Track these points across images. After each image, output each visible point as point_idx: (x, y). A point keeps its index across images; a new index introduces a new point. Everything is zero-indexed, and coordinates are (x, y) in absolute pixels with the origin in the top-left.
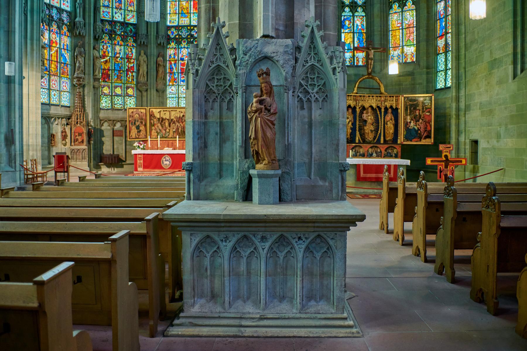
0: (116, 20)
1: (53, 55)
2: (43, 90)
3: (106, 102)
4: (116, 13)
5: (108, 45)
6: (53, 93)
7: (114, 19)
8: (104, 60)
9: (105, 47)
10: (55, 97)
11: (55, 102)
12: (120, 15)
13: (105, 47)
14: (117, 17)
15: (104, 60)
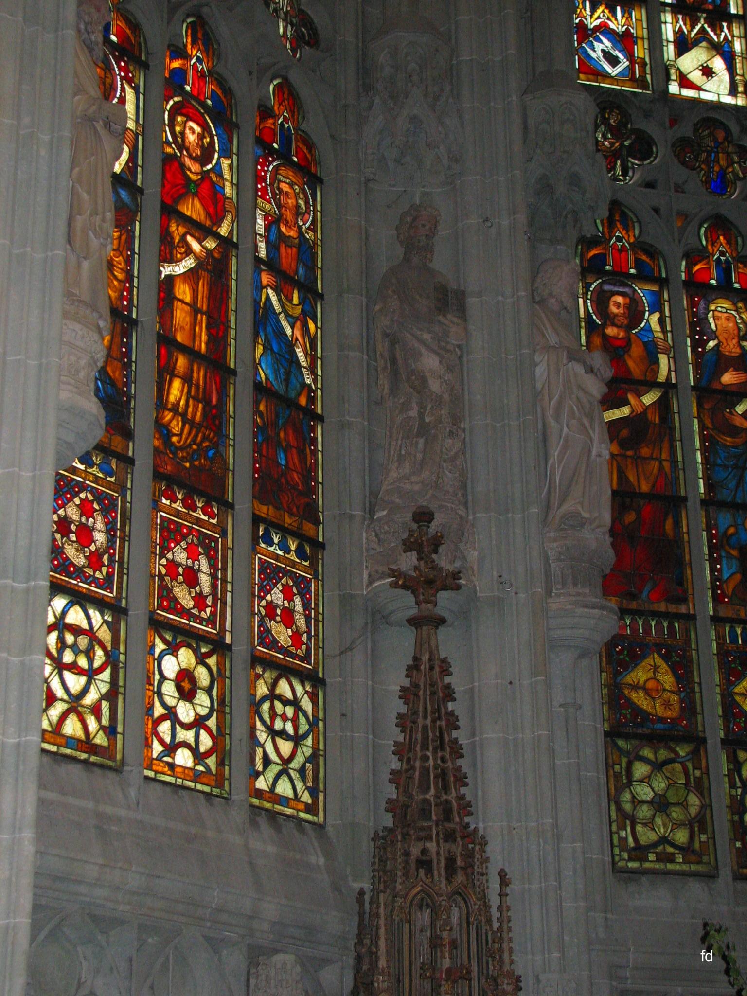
0: (687, 93)
1: (183, 292)
2: (76, 616)
3: (661, 804)
4: (683, 45)
5: (643, 291)
6: (170, 666)
7: (674, 88)
8: (625, 411)
9: (617, 304)
10: (186, 713)
11: (183, 758)
12: (718, 64)
13: (617, 304)
14: (696, 77)
15: (625, 411)
